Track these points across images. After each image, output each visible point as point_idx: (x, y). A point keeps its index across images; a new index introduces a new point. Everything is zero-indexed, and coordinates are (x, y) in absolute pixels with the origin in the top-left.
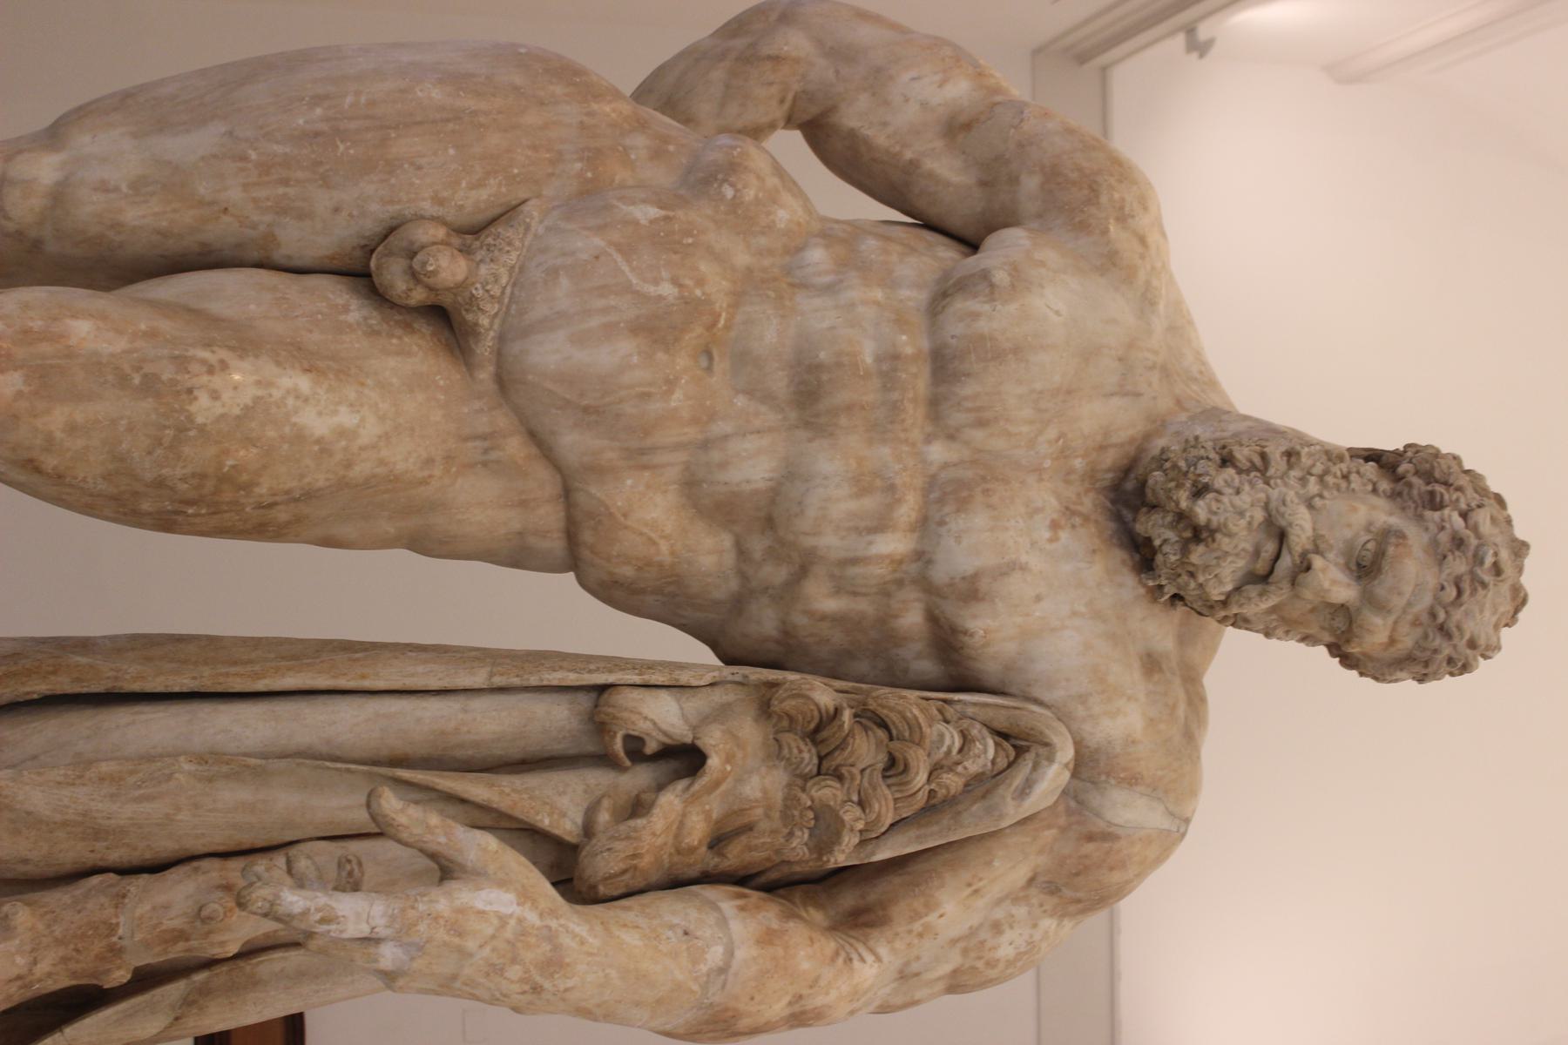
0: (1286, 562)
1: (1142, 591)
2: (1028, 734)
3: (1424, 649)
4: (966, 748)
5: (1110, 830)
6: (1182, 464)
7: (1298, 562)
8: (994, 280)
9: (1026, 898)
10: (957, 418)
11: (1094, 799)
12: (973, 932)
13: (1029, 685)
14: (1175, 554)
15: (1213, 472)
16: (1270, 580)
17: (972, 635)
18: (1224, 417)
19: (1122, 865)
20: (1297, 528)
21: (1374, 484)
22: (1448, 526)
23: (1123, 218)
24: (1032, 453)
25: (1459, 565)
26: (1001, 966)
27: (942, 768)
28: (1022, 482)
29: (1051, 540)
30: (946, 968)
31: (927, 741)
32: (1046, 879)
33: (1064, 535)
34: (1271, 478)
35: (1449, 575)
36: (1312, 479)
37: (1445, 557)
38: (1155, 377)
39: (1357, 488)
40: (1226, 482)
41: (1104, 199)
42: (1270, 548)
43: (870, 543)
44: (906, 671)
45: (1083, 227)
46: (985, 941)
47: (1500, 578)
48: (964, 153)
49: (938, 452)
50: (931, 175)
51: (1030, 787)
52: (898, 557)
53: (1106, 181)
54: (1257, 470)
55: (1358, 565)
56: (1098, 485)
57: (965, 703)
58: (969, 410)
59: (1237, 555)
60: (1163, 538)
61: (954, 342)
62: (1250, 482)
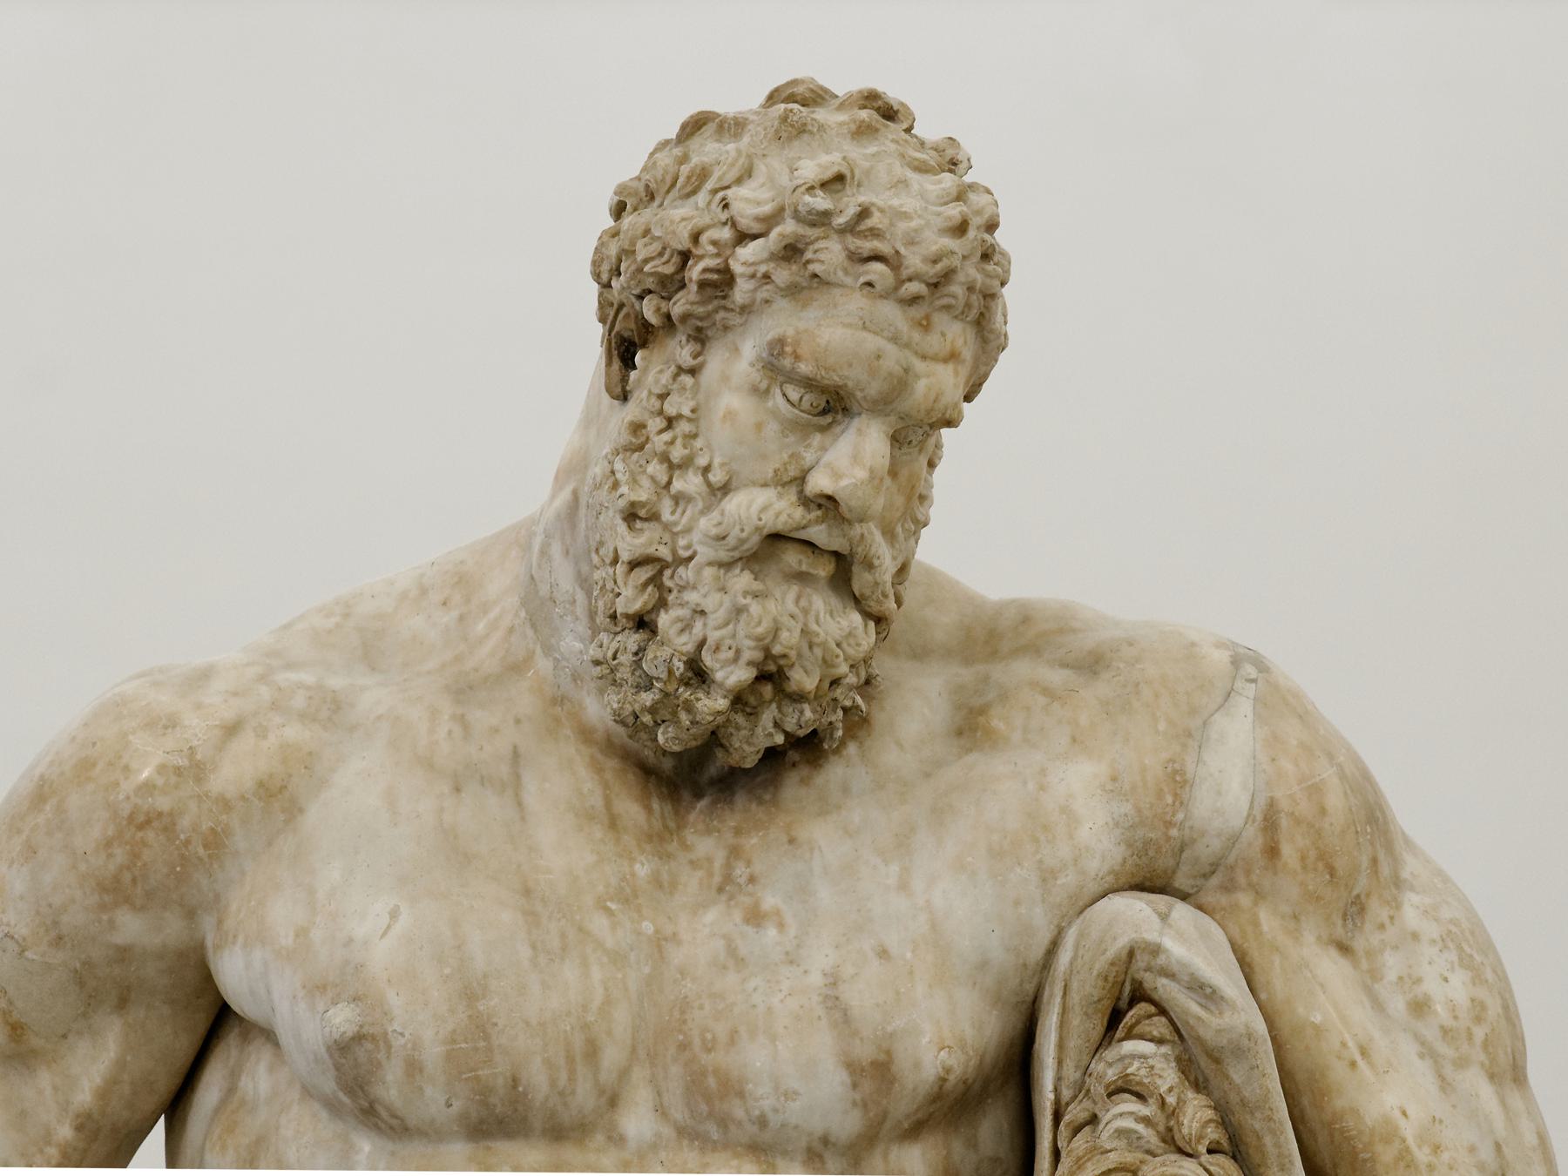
0: (819, 534)
1: (852, 749)
2: (1115, 983)
3: (968, 305)
4: (1137, 1088)
5: (1259, 817)
6: (648, 698)
7: (819, 513)
8: (349, 1034)
9: (1370, 954)
10: (584, 1097)
11: (1207, 848)
12: (1427, 1052)
13: (1025, 965)
14: (802, 712)
16: (844, 549)
17: (948, 1070)
18: (544, 590)
19: (1315, 790)
21: (680, 370)
22: (763, 269)
23: (194, 769)
24: (632, 957)
25: (829, 254)
26: (1482, 993)
27: (1170, 1129)
28: (683, 973)
29: (781, 926)
30: (1486, 1092)
31: (1130, 1158)
32: (1340, 922)
33: (769, 901)
34: (674, 552)
35: (846, 272)
36: (678, 485)
37: (815, 276)
38: (481, 718)
39: (692, 404)
41: (163, 803)
42: (793, 558)
44: (995, 1160)
45: (216, 842)
46: (1442, 1027)
47: (848, 175)
48: (65, 1036)
49: (637, 1122)
50: (103, 1094)
51: (1202, 986)
53: (128, 798)
54: (660, 573)
55: (824, 412)
56: (672, 825)
57: (1058, 1079)
58: (572, 1072)
59: (806, 612)
60: (772, 730)
61: (457, 1105)
62: (682, 589)
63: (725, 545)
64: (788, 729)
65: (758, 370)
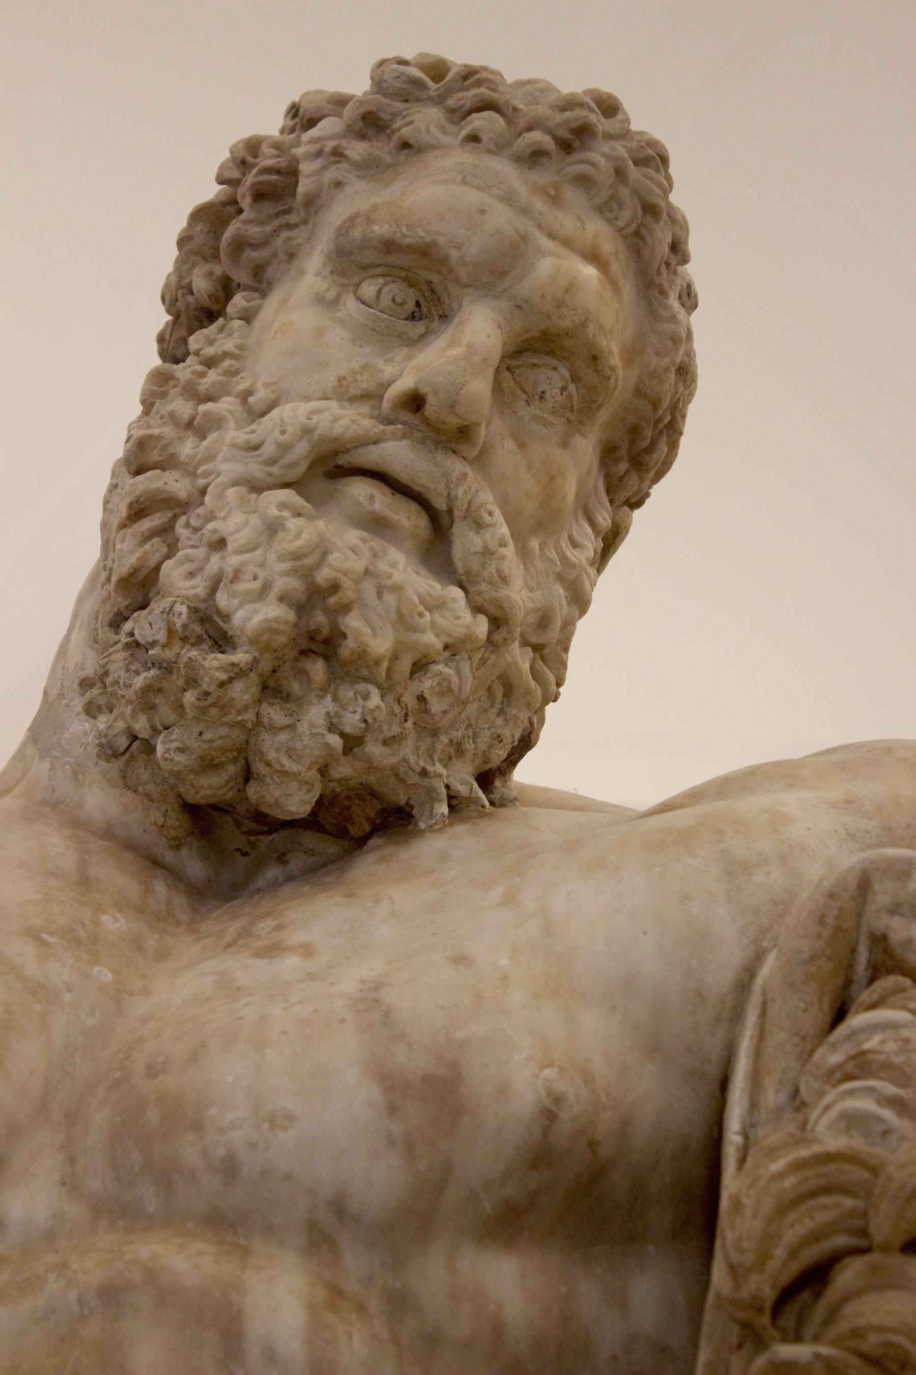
2: (838, 929)
13: (700, 995)
14: (366, 697)
15: (165, 603)
16: (440, 504)
17: (558, 1100)
20: (315, 418)
22: (332, 144)
24: (67, 997)
40: (192, 575)
43: (270, 1355)
52: (321, 1293)
55: (412, 317)
63: (259, 455)
64: (348, 730)
65: (325, 277)
